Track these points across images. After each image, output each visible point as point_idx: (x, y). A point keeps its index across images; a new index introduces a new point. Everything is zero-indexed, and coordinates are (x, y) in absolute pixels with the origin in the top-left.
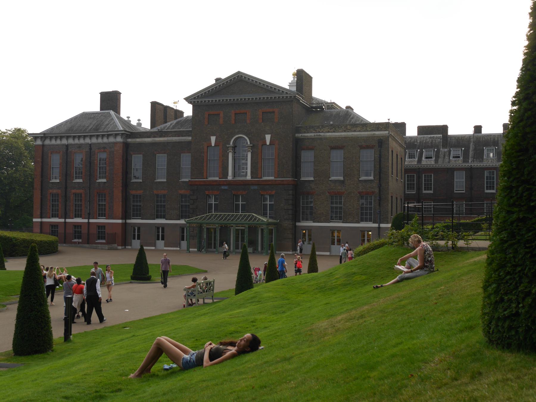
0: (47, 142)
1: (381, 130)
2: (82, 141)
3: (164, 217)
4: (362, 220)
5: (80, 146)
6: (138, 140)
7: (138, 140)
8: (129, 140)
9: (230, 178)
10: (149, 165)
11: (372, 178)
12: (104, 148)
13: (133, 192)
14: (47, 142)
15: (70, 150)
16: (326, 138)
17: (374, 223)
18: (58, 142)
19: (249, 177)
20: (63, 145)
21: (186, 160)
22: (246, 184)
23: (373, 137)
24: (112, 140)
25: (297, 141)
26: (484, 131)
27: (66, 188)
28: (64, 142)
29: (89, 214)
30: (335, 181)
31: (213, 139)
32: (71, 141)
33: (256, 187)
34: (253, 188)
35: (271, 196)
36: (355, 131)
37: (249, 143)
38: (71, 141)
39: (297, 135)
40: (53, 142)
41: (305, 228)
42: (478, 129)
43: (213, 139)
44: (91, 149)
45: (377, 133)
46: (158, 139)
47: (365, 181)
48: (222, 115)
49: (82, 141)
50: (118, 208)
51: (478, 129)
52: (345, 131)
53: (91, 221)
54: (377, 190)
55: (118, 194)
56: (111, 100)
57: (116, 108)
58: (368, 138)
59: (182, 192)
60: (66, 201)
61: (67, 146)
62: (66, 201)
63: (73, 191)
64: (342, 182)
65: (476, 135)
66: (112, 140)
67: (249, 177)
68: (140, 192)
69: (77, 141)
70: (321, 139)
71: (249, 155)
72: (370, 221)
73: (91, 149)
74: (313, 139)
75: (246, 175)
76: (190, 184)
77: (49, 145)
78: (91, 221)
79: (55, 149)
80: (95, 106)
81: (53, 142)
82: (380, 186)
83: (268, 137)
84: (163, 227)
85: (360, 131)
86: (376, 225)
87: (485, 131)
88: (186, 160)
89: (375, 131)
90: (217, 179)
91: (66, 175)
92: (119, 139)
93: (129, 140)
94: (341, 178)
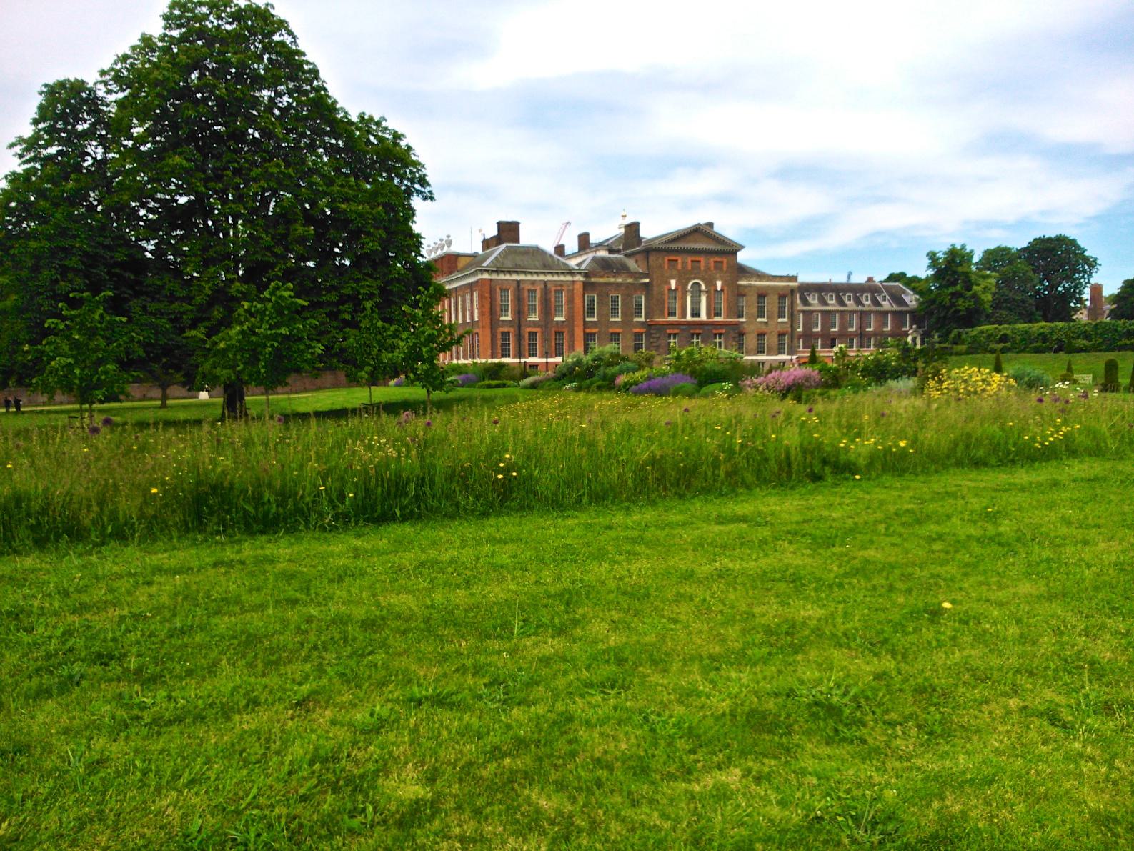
0: (494, 276)
2: (535, 277)
5: (533, 282)
11: (785, 320)
12: (561, 286)
15: (522, 286)
16: (755, 286)
18: (508, 277)
19: (704, 317)
22: (702, 324)
29: (547, 353)
30: (761, 322)
32: (522, 277)
33: (710, 327)
34: (706, 327)
37: (703, 287)
38: (522, 277)
44: (546, 286)
46: (612, 280)
48: (680, 261)
59: (637, 330)
61: (518, 282)
64: (766, 323)
66: (569, 278)
69: (529, 277)
70: (750, 286)
73: (546, 286)
78: (550, 360)
81: (502, 277)
82: (792, 326)
91: (519, 314)
94: (765, 320)
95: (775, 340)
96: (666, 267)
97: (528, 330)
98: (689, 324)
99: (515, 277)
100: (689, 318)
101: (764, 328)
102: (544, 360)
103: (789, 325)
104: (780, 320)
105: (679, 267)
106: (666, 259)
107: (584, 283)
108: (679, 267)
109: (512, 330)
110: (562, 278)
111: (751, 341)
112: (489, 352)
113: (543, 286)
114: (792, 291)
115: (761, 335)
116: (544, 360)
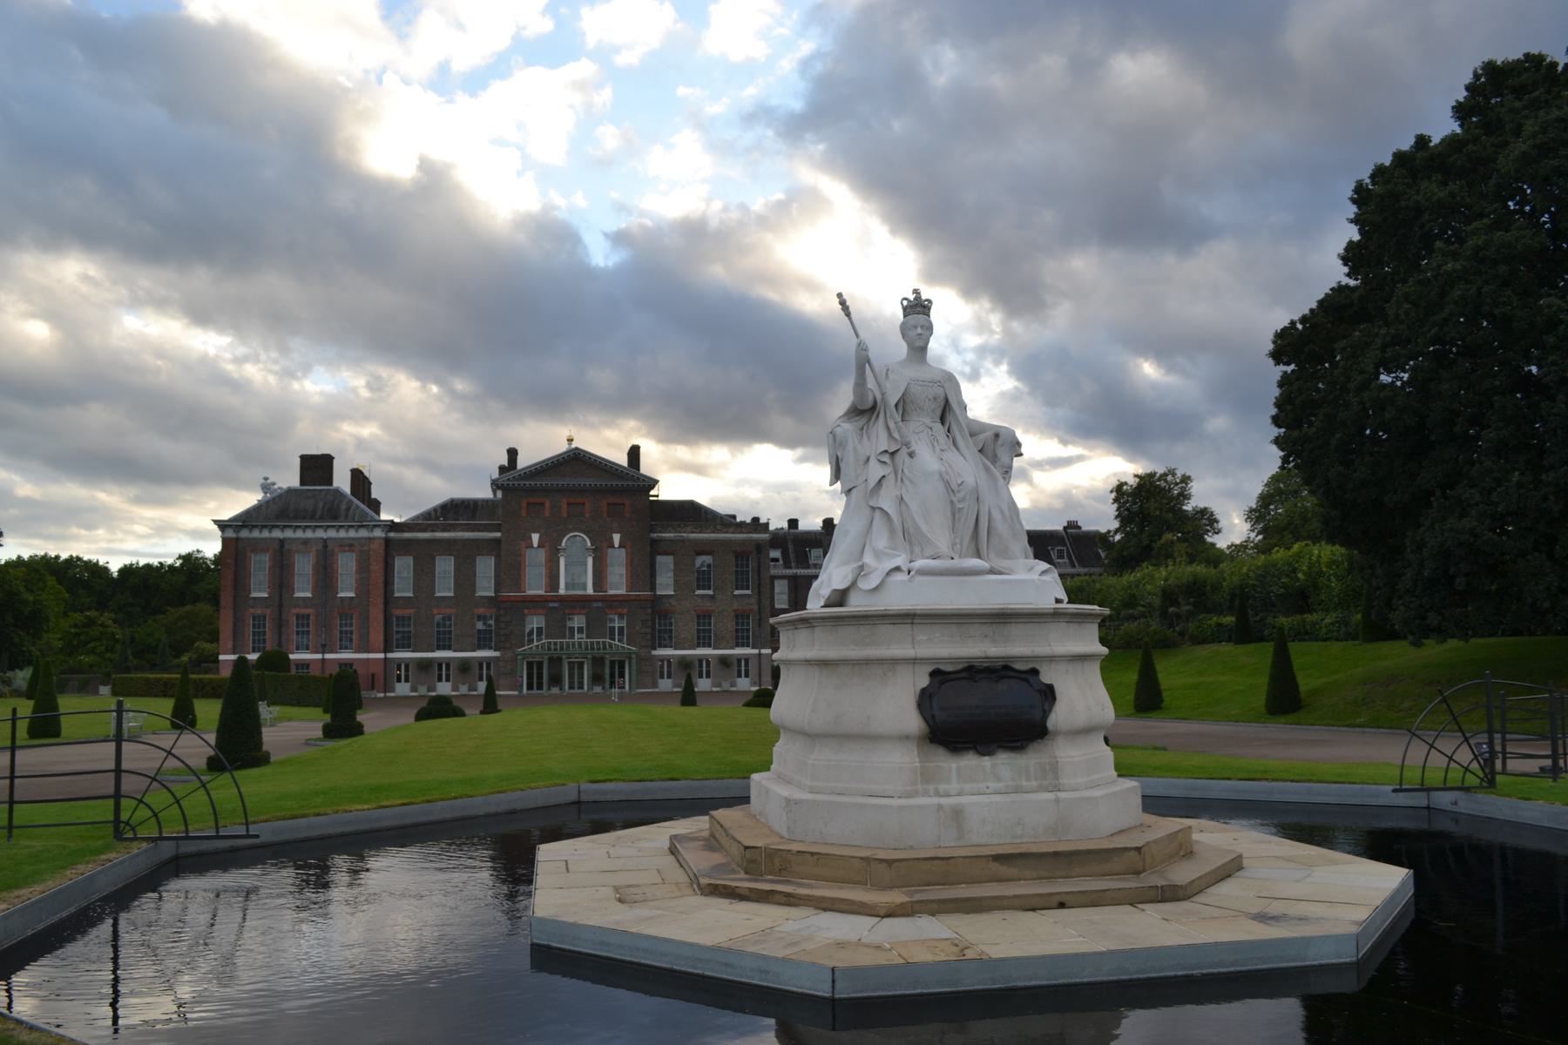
0: (244, 534)
2: (309, 534)
3: (449, 648)
5: (306, 542)
6: (407, 535)
7: (407, 535)
8: (392, 535)
9: (562, 591)
10: (424, 572)
13: (398, 612)
14: (244, 534)
15: (287, 547)
16: (689, 540)
18: (266, 534)
19: (590, 591)
20: (274, 539)
21: (485, 569)
22: (585, 600)
23: (750, 540)
24: (363, 533)
25: (654, 542)
26: (802, 526)
27: (281, 606)
28: (277, 534)
29: (324, 646)
31: (535, 538)
32: (289, 534)
35: (621, 616)
38: (289, 534)
39: (654, 535)
40: (256, 534)
41: (662, 659)
42: (793, 523)
43: (535, 538)
44: (326, 546)
47: (741, 596)
48: (547, 504)
49: (309, 534)
50: (377, 636)
51: (793, 523)
53: (328, 656)
54: (755, 607)
55: (377, 614)
56: (317, 467)
57: (328, 478)
58: (743, 542)
59: (481, 611)
60: (280, 626)
61: (282, 542)
62: (280, 626)
63: (296, 611)
64: (712, 597)
66: (363, 533)
67: (590, 591)
68: (407, 612)
69: (299, 534)
70: (683, 541)
71: (590, 561)
73: (326, 546)
74: (672, 541)
75: (585, 588)
76: (492, 601)
77: (248, 539)
78: (328, 656)
79: (257, 546)
80: (289, 478)
81: (256, 534)
82: (759, 603)
83: (616, 538)
84: (448, 661)
87: (802, 526)
88: (485, 569)
90: (542, 592)
92: (378, 533)
93: (392, 535)
95: (730, 625)
96: (524, 513)
97: (296, 611)
98: (562, 599)
99: (277, 534)
100: (562, 591)
101: (707, 605)
102: (319, 656)
103: (753, 601)
105: (547, 513)
106: (524, 505)
107: (387, 541)
108: (547, 513)
109: (268, 612)
110: (352, 534)
111: (685, 625)
112: (230, 645)
113: (320, 547)
114: (760, 548)
115: (704, 617)
116: (319, 656)
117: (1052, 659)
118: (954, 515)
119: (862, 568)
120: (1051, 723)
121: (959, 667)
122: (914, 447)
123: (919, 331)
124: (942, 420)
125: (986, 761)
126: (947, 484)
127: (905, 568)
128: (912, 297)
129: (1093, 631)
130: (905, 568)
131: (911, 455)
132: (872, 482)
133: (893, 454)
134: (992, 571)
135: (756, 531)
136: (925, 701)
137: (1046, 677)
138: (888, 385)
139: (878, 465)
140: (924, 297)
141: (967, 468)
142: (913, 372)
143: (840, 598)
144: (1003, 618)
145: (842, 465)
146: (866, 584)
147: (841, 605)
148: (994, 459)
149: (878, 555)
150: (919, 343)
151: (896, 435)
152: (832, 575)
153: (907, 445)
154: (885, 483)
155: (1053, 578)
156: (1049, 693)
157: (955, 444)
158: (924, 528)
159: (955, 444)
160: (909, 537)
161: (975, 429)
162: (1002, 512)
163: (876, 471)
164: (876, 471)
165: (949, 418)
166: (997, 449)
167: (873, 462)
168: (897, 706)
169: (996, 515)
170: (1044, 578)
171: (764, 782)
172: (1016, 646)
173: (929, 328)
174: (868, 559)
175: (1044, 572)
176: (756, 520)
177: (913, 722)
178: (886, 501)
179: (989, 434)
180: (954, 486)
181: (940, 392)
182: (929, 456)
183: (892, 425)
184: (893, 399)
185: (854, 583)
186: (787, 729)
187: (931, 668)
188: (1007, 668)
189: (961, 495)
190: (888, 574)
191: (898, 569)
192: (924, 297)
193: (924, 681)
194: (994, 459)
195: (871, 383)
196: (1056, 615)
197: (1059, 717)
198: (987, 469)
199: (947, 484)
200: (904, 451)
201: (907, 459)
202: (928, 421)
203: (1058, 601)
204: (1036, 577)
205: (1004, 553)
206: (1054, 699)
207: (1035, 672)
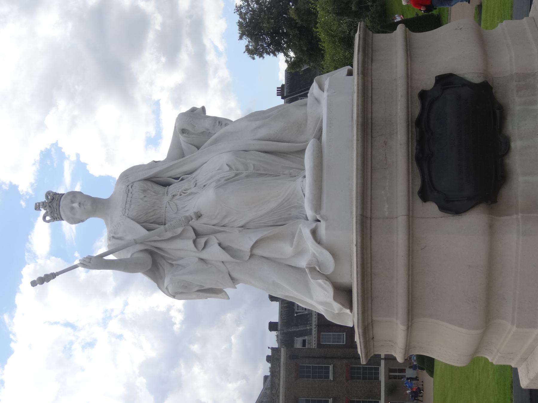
1: (280, 356)
4: (377, 378)
11: (331, 367)
17: (380, 365)
26: (276, 319)
36: (279, 385)
42: (273, 326)
45: (282, 359)
47: (334, 373)
51: (273, 326)
52: (278, 396)
65: (279, 328)
72: (378, 369)
85: (279, 379)
86: (383, 362)
87: (276, 319)
89: (280, 363)
104: (331, 378)
114: (293, 356)
117: (409, 77)
118: (261, 175)
119: (312, 269)
120: (477, 80)
121: (417, 171)
122: (191, 213)
123: (76, 205)
124: (166, 185)
125: (516, 145)
126: (229, 181)
127: (314, 225)
128: (43, 212)
129: (380, 39)
130: (314, 225)
131: (199, 216)
132: (225, 256)
133: (198, 234)
134: (319, 138)
135: (279, 359)
136: (452, 206)
137: (427, 82)
138: (130, 237)
139: (208, 250)
140: (43, 199)
141: (215, 162)
142: (117, 213)
143: (343, 293)
144: (368, 127)
145: (207, 286)
146: (330, 264)
147: (349, 291)
148: (207, 134)
149: (299, 252)
150: (88, 206)
151: (179, 230)
152: (319, 299)
153: (188, 219)
154: (226, 244)
155: (327, 79)
156: (446, 81)
157: (190, 173)
158: (273, 205)
159: (190, 173)
160: (282, 220)
161: (178, 152)
162: (259, 127)
163: (213, 252)
164: (213, 252)
165: (165, 178)
166: (195, 129)
167: (205, 255)
168: (456, 237)
169: (263, 133)
170: (326, 87)
171: (532, 375)
172: (397, 112)
173: (73, 195)
174: (303, 263)
175: (321, 88)
176: (269, 359)
177: (475, 219)
178: (245, 243)
179: (182, 138)
180: (232, 174)
181: (137, 186)
182: (202, 200)
183: (169, 235)
184: (143, 232)
185: (328, 278)
186: (476, 351)
187: (418, 201)
188: (419, 122)
189: (240, 167)
190: (318, 241)
191: (314, 232)
192: (43, 199)
193: (432, 208)
194: (207, 134)
195: (126, 255)
196: (365, 74)
197: (468, 68)
198: (216, 141)
199: (229, 181)
200: (195, 223)
201: (203, 220)
202: (167, 199)
203: (350, 73)
204: (325, 94)
205: (301, 126)
206: (450, 75)
207: (423, 95)
